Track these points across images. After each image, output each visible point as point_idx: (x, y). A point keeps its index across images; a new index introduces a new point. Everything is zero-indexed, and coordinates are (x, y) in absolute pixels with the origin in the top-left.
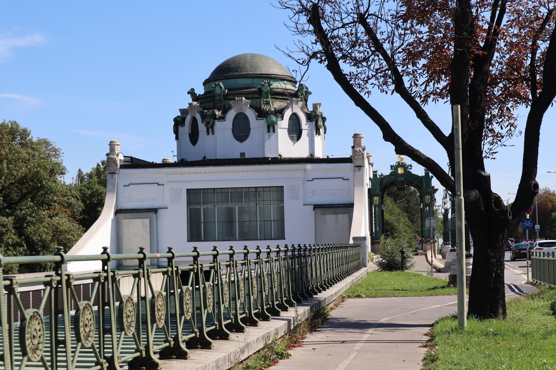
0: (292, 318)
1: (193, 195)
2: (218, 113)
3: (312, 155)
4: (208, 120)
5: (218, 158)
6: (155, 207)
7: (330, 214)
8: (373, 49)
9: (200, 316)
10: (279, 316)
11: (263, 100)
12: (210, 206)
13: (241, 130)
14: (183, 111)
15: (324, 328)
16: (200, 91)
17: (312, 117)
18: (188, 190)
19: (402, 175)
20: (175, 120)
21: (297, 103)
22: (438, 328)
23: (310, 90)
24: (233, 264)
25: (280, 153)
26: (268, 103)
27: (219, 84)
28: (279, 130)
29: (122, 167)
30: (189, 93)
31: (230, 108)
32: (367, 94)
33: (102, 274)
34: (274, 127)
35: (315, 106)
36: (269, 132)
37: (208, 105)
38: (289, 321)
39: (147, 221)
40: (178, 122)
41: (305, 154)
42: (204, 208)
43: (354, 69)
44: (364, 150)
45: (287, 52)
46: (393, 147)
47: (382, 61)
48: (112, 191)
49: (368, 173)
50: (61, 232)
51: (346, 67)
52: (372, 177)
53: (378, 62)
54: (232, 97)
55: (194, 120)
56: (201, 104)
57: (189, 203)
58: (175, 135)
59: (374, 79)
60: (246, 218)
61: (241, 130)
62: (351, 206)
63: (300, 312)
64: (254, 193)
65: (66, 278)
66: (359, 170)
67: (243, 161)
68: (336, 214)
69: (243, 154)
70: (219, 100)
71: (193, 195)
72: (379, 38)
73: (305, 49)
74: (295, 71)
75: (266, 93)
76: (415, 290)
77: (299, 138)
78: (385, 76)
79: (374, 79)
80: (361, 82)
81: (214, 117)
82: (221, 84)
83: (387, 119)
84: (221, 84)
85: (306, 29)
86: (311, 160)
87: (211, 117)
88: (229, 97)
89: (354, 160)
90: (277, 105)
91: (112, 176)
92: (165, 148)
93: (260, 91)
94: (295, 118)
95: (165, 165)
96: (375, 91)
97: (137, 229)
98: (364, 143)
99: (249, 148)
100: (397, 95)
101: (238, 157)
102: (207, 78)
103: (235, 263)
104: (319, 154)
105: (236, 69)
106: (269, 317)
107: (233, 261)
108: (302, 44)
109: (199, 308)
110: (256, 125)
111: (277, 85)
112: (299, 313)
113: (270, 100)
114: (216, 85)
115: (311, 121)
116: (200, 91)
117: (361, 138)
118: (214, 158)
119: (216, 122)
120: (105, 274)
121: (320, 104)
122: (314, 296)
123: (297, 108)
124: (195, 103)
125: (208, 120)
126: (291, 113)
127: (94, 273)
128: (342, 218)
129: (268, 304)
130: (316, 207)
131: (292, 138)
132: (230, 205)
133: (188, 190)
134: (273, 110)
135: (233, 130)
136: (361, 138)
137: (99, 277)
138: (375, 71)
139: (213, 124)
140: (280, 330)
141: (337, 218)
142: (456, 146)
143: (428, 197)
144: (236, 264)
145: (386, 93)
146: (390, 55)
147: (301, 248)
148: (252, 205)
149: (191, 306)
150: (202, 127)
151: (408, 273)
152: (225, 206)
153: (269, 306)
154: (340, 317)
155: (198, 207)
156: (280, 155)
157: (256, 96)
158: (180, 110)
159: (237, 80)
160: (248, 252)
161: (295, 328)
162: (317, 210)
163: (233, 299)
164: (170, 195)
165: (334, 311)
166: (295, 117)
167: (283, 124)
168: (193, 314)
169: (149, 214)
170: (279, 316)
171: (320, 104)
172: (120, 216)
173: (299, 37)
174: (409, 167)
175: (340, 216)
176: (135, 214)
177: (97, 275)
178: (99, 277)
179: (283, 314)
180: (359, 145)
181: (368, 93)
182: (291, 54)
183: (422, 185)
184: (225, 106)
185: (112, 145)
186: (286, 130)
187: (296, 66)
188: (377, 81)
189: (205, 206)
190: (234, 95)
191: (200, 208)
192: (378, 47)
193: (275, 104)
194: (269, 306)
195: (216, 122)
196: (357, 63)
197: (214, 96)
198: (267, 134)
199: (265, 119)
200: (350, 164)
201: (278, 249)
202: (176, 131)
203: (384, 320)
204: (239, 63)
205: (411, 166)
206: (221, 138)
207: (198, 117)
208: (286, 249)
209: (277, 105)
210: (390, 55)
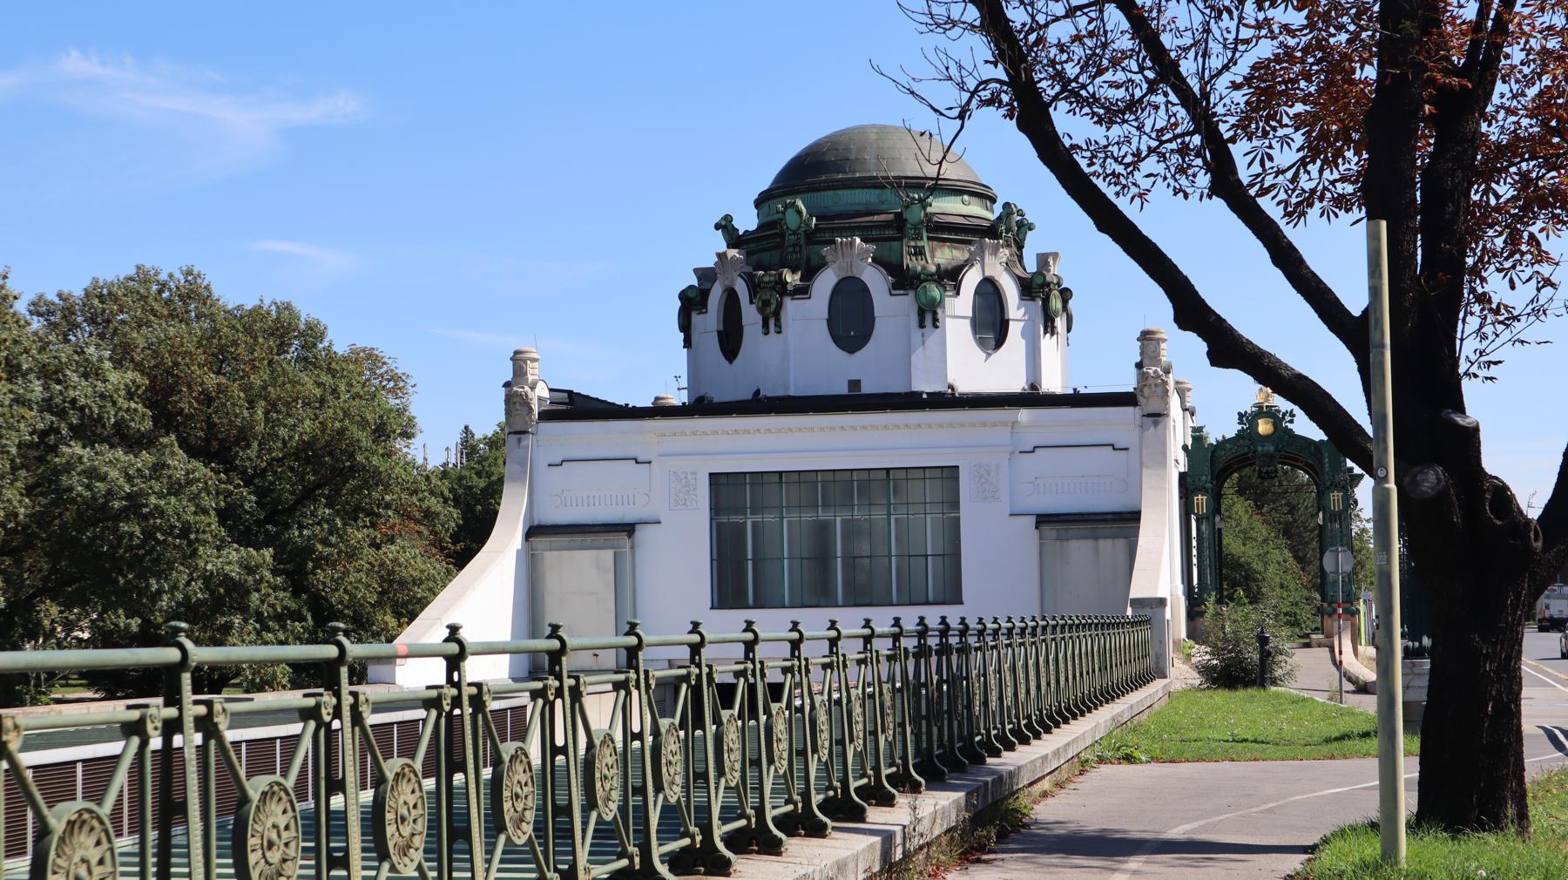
0: (898, 829)
1: (727, 490)
2: (792, 278)
3: (1033, 387)
4: (766, 296)
5: (792, 393)
6: (629, 518)
7: (1078, 538)
8: (1150, 75)
9: (642, 812)
10: (863, 820)
11: (908, 245)
12: (770, 518)
13: (851, 322)
14: (704, 275)
15: (1003, 852)
16: (747, 221)
17: (1035, 288)
18: (713, 477)
19: (1267, 437)
20: (683, 296)
21: (995, 252)
22: (1326, 858)
23: (1030, 218)
24: (754, 671)
25: (950, 380)
26: (919, 252)
27: (793, 205)
28: (948, 320)
29: (546, 416)
30: (717, 227)
31: (823, 264)
32: (1137, 200)
33: (445, 691)
34: (935, 313)
35: (1043, 260)
36: (922, 325)
37: (766, 257)
38: (888, 838)
39: (608, 555)
40: (691, 302)
41: (1016, 383)
42: (754, 523)
43: (1098, 133)
44: (1167, 371)
45: (904, 80)
46: (1202, 346)
47: (1175, 109)
48: (519, 479)
49: (1178, 433)
50: (402, 583)
51: (1071, 125)
52: (1189, 442)
53: (1166, 111)
54: (827, 236)
55: (731, 295)
56: (748, 254)
57: (715, 509)
58: (682, 335)
59: (1154, 158)
60: (864, 548)
61: (851, 322)
63: (934, 809)
64: (884, 483)
65: (351, 700)
66: (1156, 424)
67: (855, 401)
68: (1096, 538)
69: (855, 384)
70: (794, 246)
71: (727, 490)
72: (1168, 46)
73: (954, 71)
74: (927, 136)
75: (916, 227)
76: (1290, 743)
77: (999, 342)
78: (1183, 151)
79: (1154, 158)
80: (1120, 169)
81: (781, 288)
82: (800, 204)
83: (1185, 268)
84: (800, 204)
85: (955, 16)
86: (1033, 398)
87: (773, 288)
88: (819, 237)
89: (1141, 399)
90: (945, 256)
91: (519, 440)
92: (657, 367)
93: (899, 223)
94: (989, 288)
95: (660, 411)
96: (1161, 193)
97: (580, 575)
99: (871, 368)
100: (1219, 203)
101: (844, 390)
102: (765, 187)
103: (758, 666)
104: (1052, 383)
105: (842, 163)
106: (825, 825)
107: (753, 662)
108: (943, 57)
109: (641, 791)
110: (890, 308)
111: (946, 207)
112: (921, 813)
113: (924, 243)
114: (786, 207)
115: (1033, 299)
116: (747, 221)
117: (1159, 341)
118: (780, 393)
119: (788, 303)
120: (454, 692)
121: (1055, 255)
122: (989, 760)
123: (996, 266)
124: (733, 253)
125: (766, 296)
126: (980, 278)
127: (428, 688)
128: (1110, 548)
129: (830, 787)
130: (1043, 520)
131: (981, 343)
132: (823, 515)
133: (713, 477)
134: (933, 269)
135: (831, 323)
136: (1159, 341)
137: (439, 698)
138: (1154, 135)
139: (780, 306)
140: (851, 865)
141: (1096, 550)
142: (1374, 336)
143: (1336, 496)
144: (762, 670)
145: (1186, 196)
146: (1196, 90)
147: (967, 627)
148: (878, 514)
149: (617, 782)
150: (750, 315)
151: (1277, 695)
152: (808, 517)
153: (831, 793)
154: (1052, 818)
155: (739, 519)
156: (951, 387)
157: (889, 233)
158: (696, 271)
159: (840, 192)
160: (756, 640)
161: (907, 855)
162: (1045, 528)
163: (697, 776)
164: (667, 488)
165: (1050, 801)
166: (990, 289)
167: (960, 307)
168: (623, 809)
169: (612, 537)
170: (863, 820)
171: (1055, 255)
172: (540, 542)
173: (938, 39)
174: (1288, 418)
175: (1105, 544)
176: (578, 539)
177: (434, 693)
178: (439, 698)
179: (876, 816)
180: (1156, 359)
181: (1140, 195)
182: (915, 87)
183: (1321, 464)
184: (809, 260)
185: (519, 360)
186: (967, 323)
187: (927, 121)
188: (1162, 165)
189: (758, 518)
190: (832, 232)
192: (1166, 70)
193: (938, 253)
194: (831, 793)
195: (788, 303)
196: (1109, 115)
197: (782, 235)
198: (916, 333)
199: (911, 293)
200: (1130, 409)
201: (867, 631)
202: (685, 326)
203: (1177, 833)
204: (847, 149)
205: (1292, 415)
206: (800, 345)
207: (741, 288)
208: (896, 629)
209: (945, 256)
210: (1196, 90)
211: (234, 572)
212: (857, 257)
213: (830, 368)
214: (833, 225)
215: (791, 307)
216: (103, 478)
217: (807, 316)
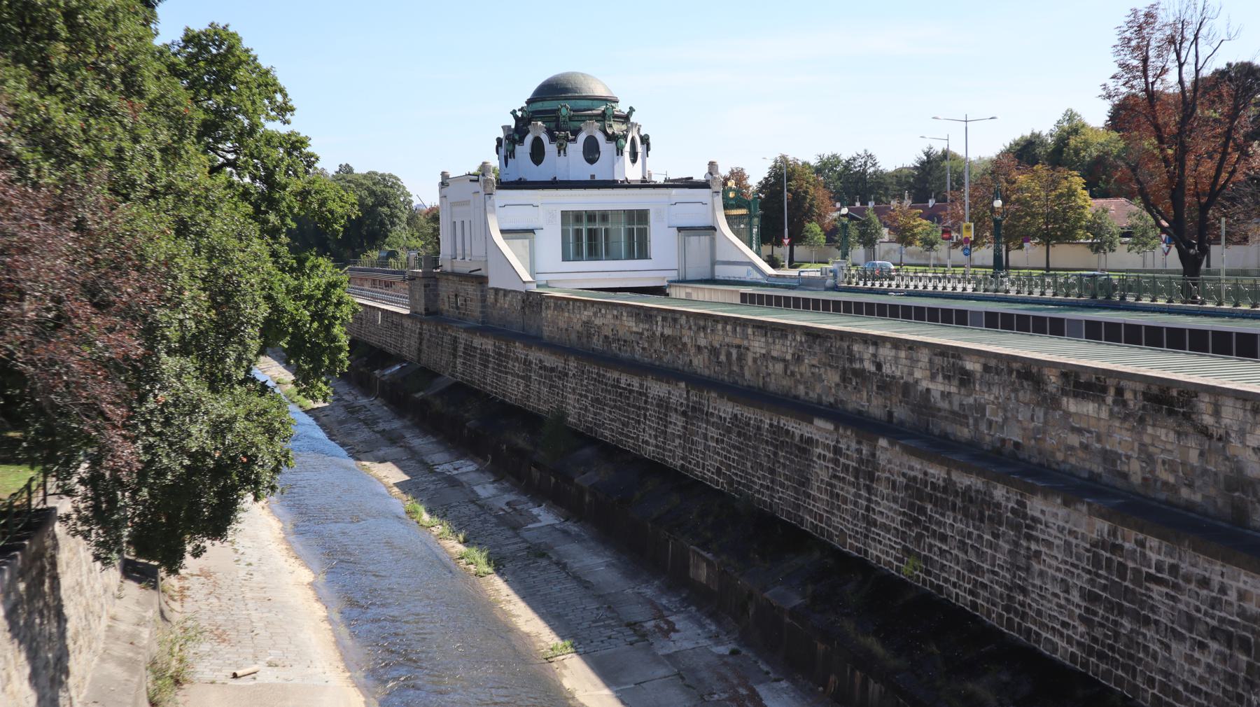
1: (565, 214)
13: (591, 152)
26: (611, 126)
42: (590, 231)
61: (591, 152)
62: (713, 229)
69: (593, 176)
71: (565, 214)
99: (599, 171)
102: (529, 95)
128: (705, 240)
130: (680, 229)
150: (550, 148)
169: (527, 235)
207: (545, 138)
213: (582, 170)
214: (579, 117)
215: (570, 146)
217: (576, 149)
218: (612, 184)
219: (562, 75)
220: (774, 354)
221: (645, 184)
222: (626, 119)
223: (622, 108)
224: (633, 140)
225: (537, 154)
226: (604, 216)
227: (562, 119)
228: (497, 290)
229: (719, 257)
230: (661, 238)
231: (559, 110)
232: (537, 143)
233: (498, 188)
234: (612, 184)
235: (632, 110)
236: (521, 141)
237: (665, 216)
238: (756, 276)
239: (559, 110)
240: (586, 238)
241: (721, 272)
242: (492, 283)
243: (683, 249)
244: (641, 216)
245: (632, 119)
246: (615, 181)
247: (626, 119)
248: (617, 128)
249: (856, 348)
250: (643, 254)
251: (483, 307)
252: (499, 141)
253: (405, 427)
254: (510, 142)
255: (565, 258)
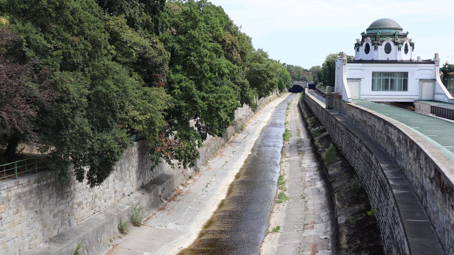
1: (374, 74)
13: (388, 49)
16: (366, 33)
19: (447, 68)
26: (397, 39)
61: (388, 49)
62: (435, 80)
69: (388, 59)
71: (374, 74)
98: (439, 57)
99: (391, 57)
101: (386, 59)
102: (367, 28)
110: (394, 47)
111: (400, 32)
128: (431, 84)
130: (420, 80)
135: (385, 49)
150: (372, 48)
191: (388, 79)
197: (376, 36)
211: (274, 82)
212: (390, 41)
215: (379, 47)
216: (260, 68)
217: (381, 48)
218: (395, 62)
219: (380, 20)
220: (379, 129)
221: (411, 62)
222: (405, 36)
223: (404, 31)
224: (406, 44)
225: (367, 50)
226: (392, 74)
227: (377, 37)
228: (343, 101)
229: (437, 91)
230: (412, 82)
231: (376, 33)
232: (367, 45)
233: (348, 62)
234: (395, 62)
235: (407, 33)
236: (362, 45)
237: (415, 75)
238: (446, 100)
239: (376, 33)
240: (386, 81)
241: (437, 97)
242: (344, 98)
243: (421, 88)
244: (405, 74)
245: (408, 37)
246: (397, 61)
247: (405, 36)
248: (399, 40)
249: (389, 128)
250: (405, 88)
251: (340, 107)
252: (356, 44)
253: (308, 150)
254: (357, 46)
255: (373, 89)
